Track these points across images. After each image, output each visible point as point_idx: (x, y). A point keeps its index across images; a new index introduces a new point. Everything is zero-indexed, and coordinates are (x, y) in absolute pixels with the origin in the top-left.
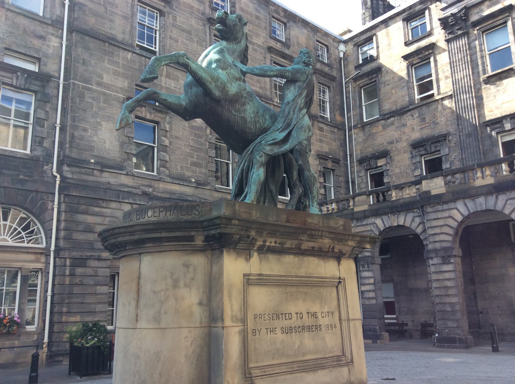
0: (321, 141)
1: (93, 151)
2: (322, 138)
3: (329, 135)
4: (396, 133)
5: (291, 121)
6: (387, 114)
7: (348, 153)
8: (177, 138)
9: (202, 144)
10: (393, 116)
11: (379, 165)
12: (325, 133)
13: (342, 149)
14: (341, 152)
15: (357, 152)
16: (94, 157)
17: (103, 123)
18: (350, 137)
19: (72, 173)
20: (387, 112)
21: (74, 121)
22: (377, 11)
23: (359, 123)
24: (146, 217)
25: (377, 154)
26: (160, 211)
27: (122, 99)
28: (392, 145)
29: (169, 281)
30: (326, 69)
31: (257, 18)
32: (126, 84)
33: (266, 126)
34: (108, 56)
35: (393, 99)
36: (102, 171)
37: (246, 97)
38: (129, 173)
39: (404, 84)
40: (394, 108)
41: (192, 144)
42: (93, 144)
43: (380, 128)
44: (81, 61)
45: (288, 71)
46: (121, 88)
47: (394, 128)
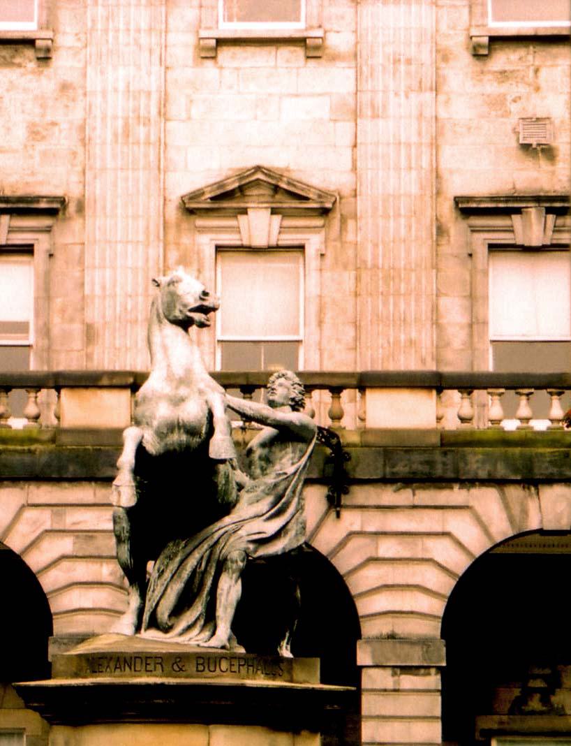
26: (240, 665)
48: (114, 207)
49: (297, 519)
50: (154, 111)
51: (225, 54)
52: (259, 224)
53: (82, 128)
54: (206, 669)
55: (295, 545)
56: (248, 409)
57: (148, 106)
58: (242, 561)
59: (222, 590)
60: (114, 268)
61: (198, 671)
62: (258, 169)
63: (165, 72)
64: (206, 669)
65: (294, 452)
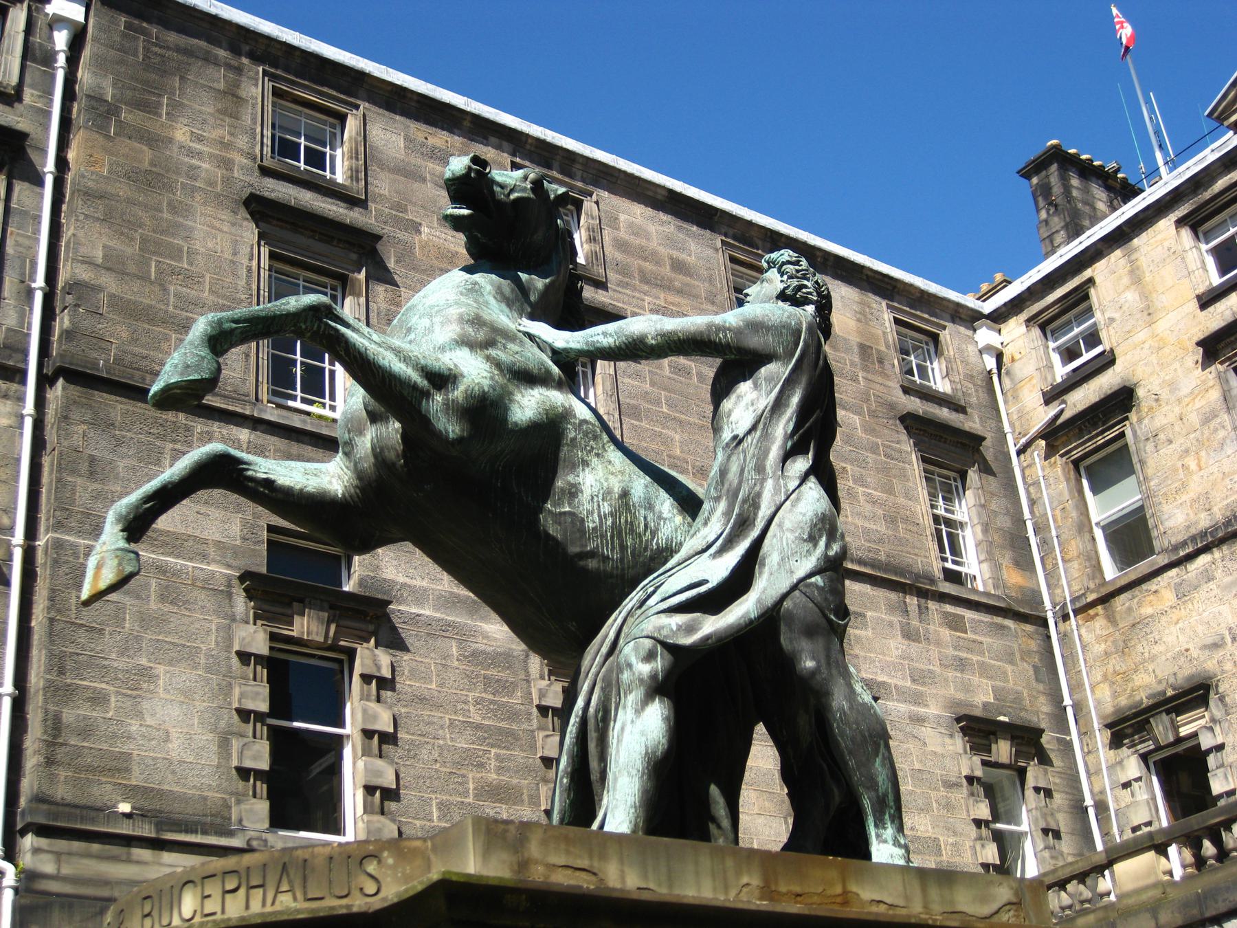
0: (961, 665)
1: (128, 770)
2: (964, 655)
3: (987, 640)
4: (1225, 609)
5: (756, 506)
6: (1184, 544)
7: (1067, 701)
8: (421, 700)
9: (513, 716)
10: (1206, 549)
11: (1184, 731)
12: (970, 635)
13: (1041, 687)
14: (1042, 699)
15: (1098, 693)
16: (130, 792)
17: (160, 669)
18: (1065, 638)
19: (58, 855)
20: (1181, 538)
21: (61, 672)
22: (1087, 209)
23: (1092, 586)
25: (1170, 693)
27: (223, 580)
28: (1219, 654)
30: (944, 414)
31: (679, 267)
32: (236, 529)
33: (662, 543)
34: (174, 441)
35: (1195, 487)
36: (158, 845)
37: (574, 439)
38: (255, 844)
39: (1221, 434)
40: (1204, 522)
41: (476, 718)
42: (125, 749)
43: (1169, 597)
44: (84, 467)
45: (724, 329)
46: (219, 545)
47: (1216, 591)
49: (780, 525)
55: (784, 585)
56: (600, 338)
58: (650, 657)
65: (756, 386)
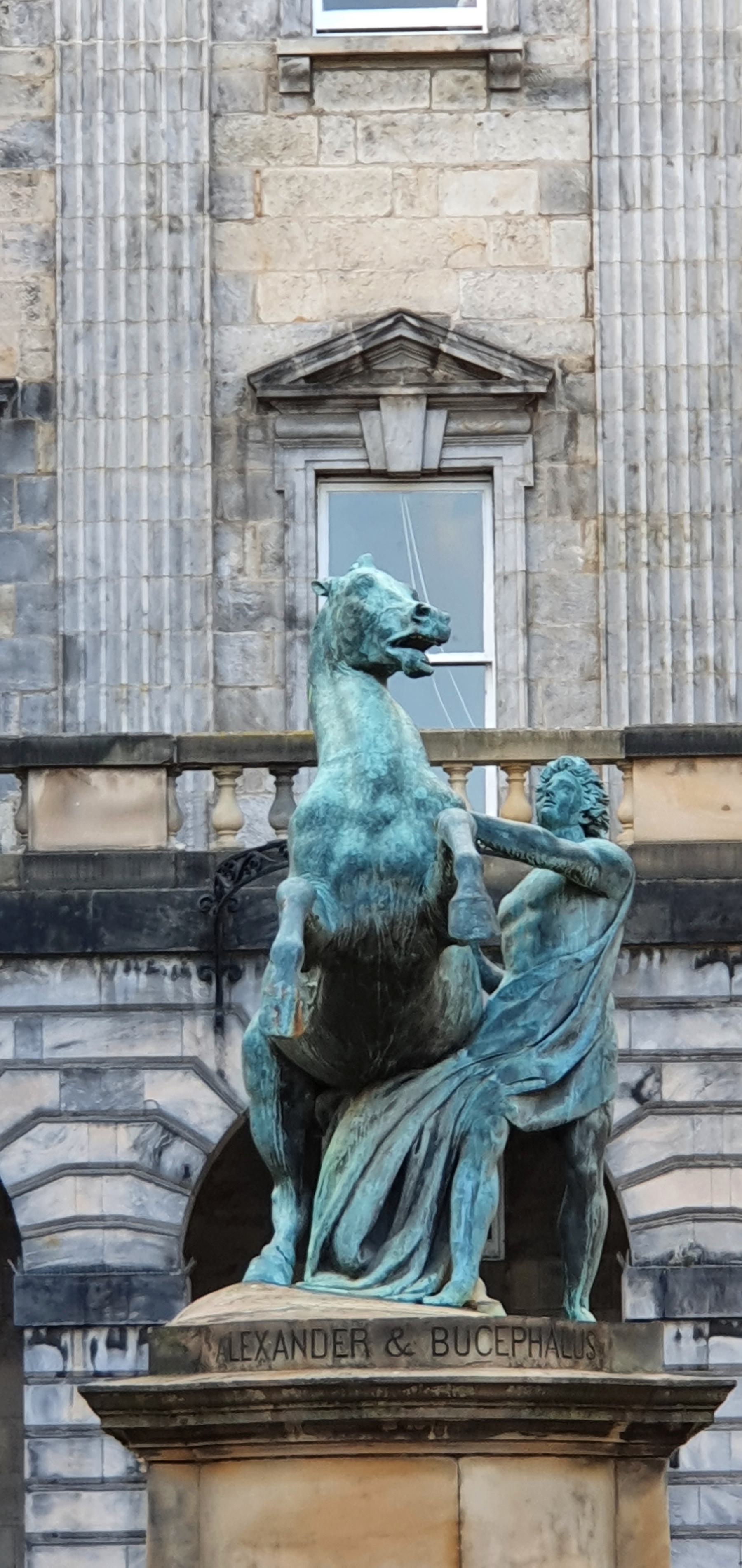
24: (473, 1350)
26: (515, 1341)
29: (548, 1537)
48: (113, 400)
50: (187, 202)
51: (329, 82)
52: (403, 432)
53: (47, 242)
54: (452, 1350)
57: (174, 195)
59: (462, 1191)
60: (114, 520)
61: (435, 1354)
62: (399, 316)
63: (212, 126)
64: (452, 1350)
